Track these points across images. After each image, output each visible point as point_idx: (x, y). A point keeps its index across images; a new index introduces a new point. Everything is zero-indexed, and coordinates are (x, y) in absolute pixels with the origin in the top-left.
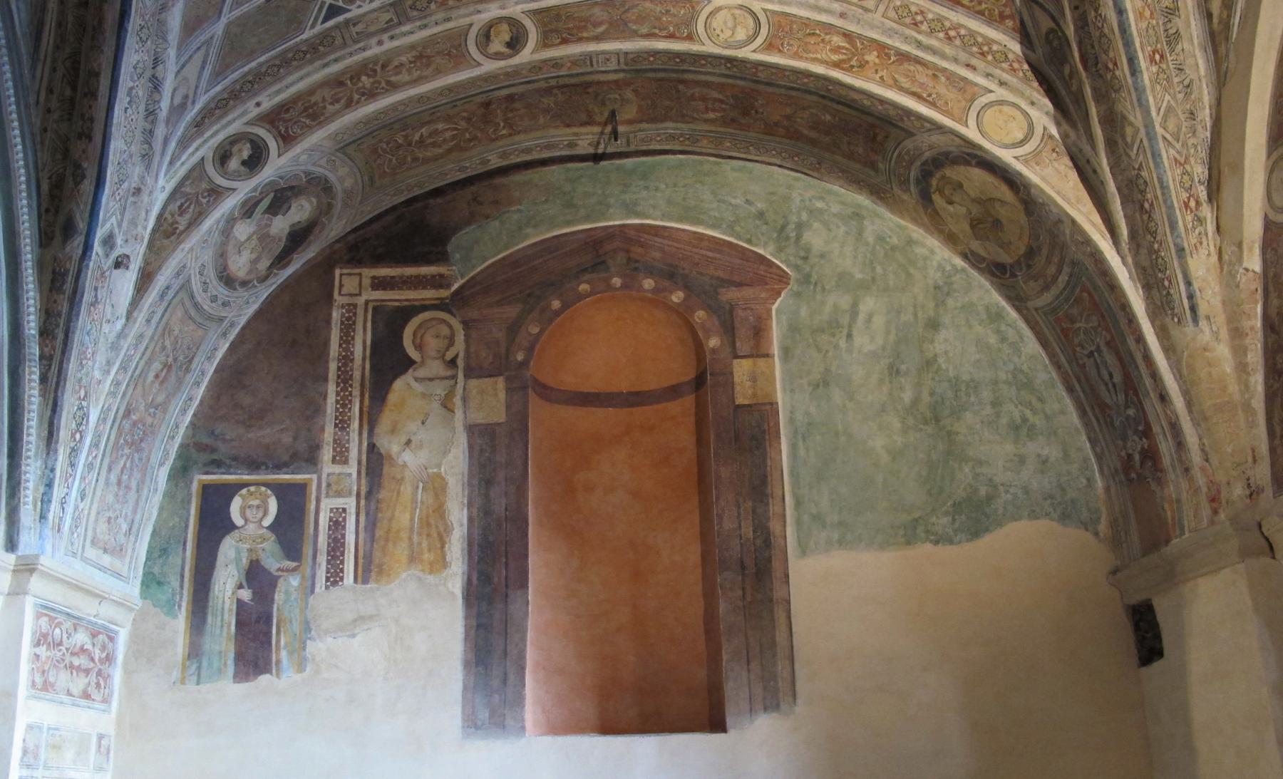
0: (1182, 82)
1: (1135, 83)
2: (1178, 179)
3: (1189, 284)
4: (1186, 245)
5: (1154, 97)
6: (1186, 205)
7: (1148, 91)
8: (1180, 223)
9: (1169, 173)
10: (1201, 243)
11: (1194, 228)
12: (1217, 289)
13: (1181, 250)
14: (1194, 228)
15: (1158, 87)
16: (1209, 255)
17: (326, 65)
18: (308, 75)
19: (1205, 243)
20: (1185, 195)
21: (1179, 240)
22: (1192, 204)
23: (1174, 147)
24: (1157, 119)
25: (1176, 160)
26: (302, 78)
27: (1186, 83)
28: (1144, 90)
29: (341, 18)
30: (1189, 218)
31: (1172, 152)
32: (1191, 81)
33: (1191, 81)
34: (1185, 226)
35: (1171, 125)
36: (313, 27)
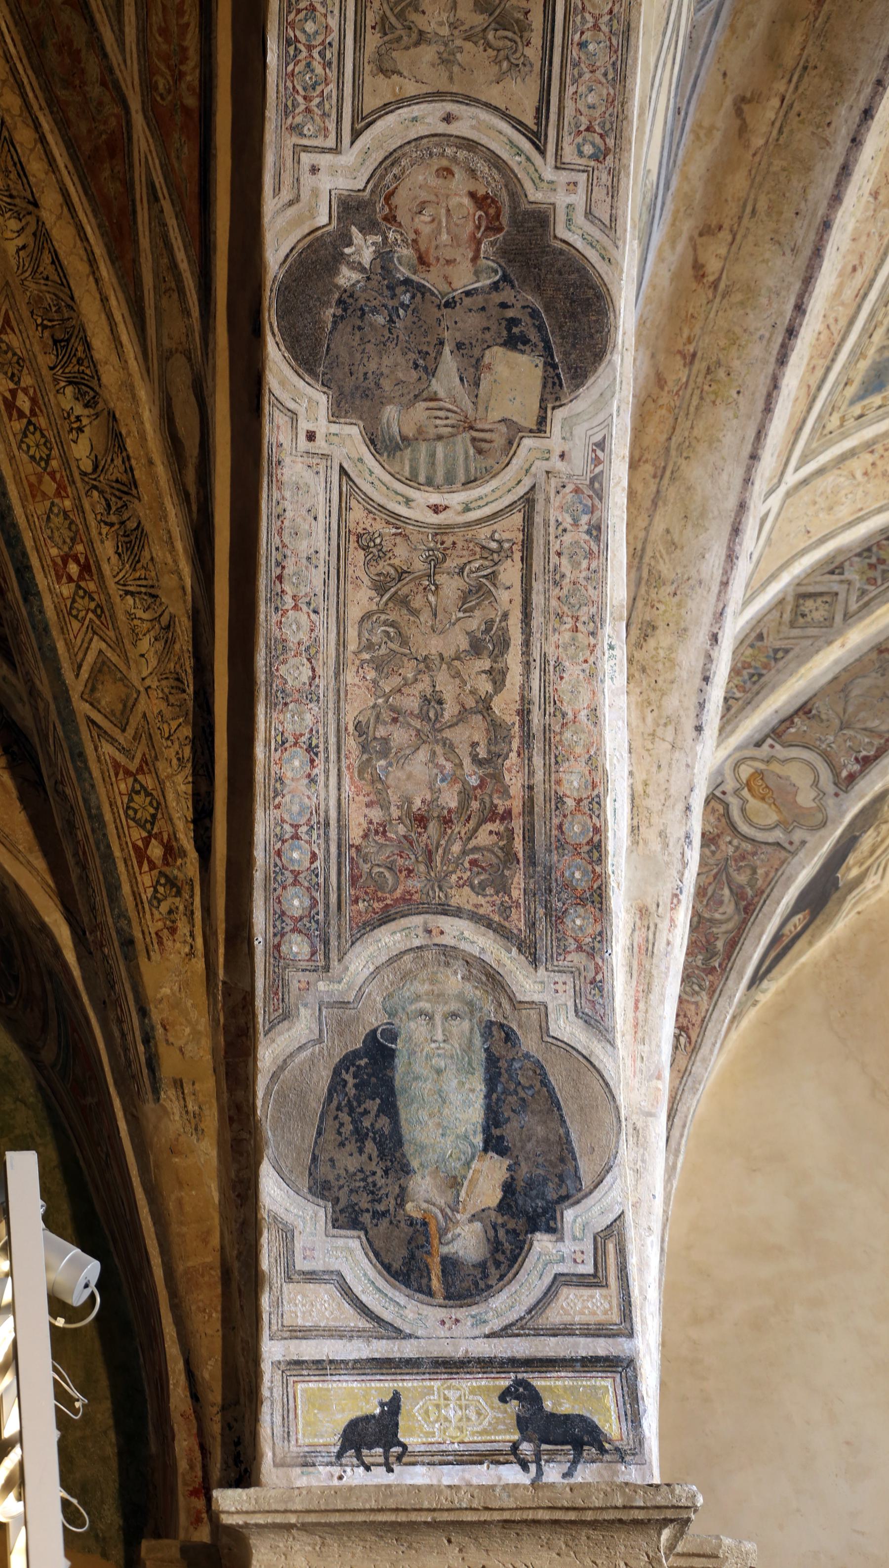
0: (158, 619)
1: (31, 614)
2: (121, 802)
3: (143, 1012)
4: (138, 935)
5: (68, 644)
6: (141, 854)
7: (55, 633)
8: (126, 889)
9: (102, 790)
10: (173, 931)
11: (156, 900)
12: (203, 1024)
13: (128, 943)
14: (156, 900)
15: (76, 625)
16: (191, 954)
19: (183, 928)
20: (137, 835)
21: (123, 923)
22: (156, 851)
23: (113, 741)
24: (76, 686)
25: (117, 765)
27: (165, 620)
28: (46, 630)
30: (146, 880)
31: (107, 749)
32: (172, 617)
33: (172, 617)
34: (136, 895)
35: (108, 695)
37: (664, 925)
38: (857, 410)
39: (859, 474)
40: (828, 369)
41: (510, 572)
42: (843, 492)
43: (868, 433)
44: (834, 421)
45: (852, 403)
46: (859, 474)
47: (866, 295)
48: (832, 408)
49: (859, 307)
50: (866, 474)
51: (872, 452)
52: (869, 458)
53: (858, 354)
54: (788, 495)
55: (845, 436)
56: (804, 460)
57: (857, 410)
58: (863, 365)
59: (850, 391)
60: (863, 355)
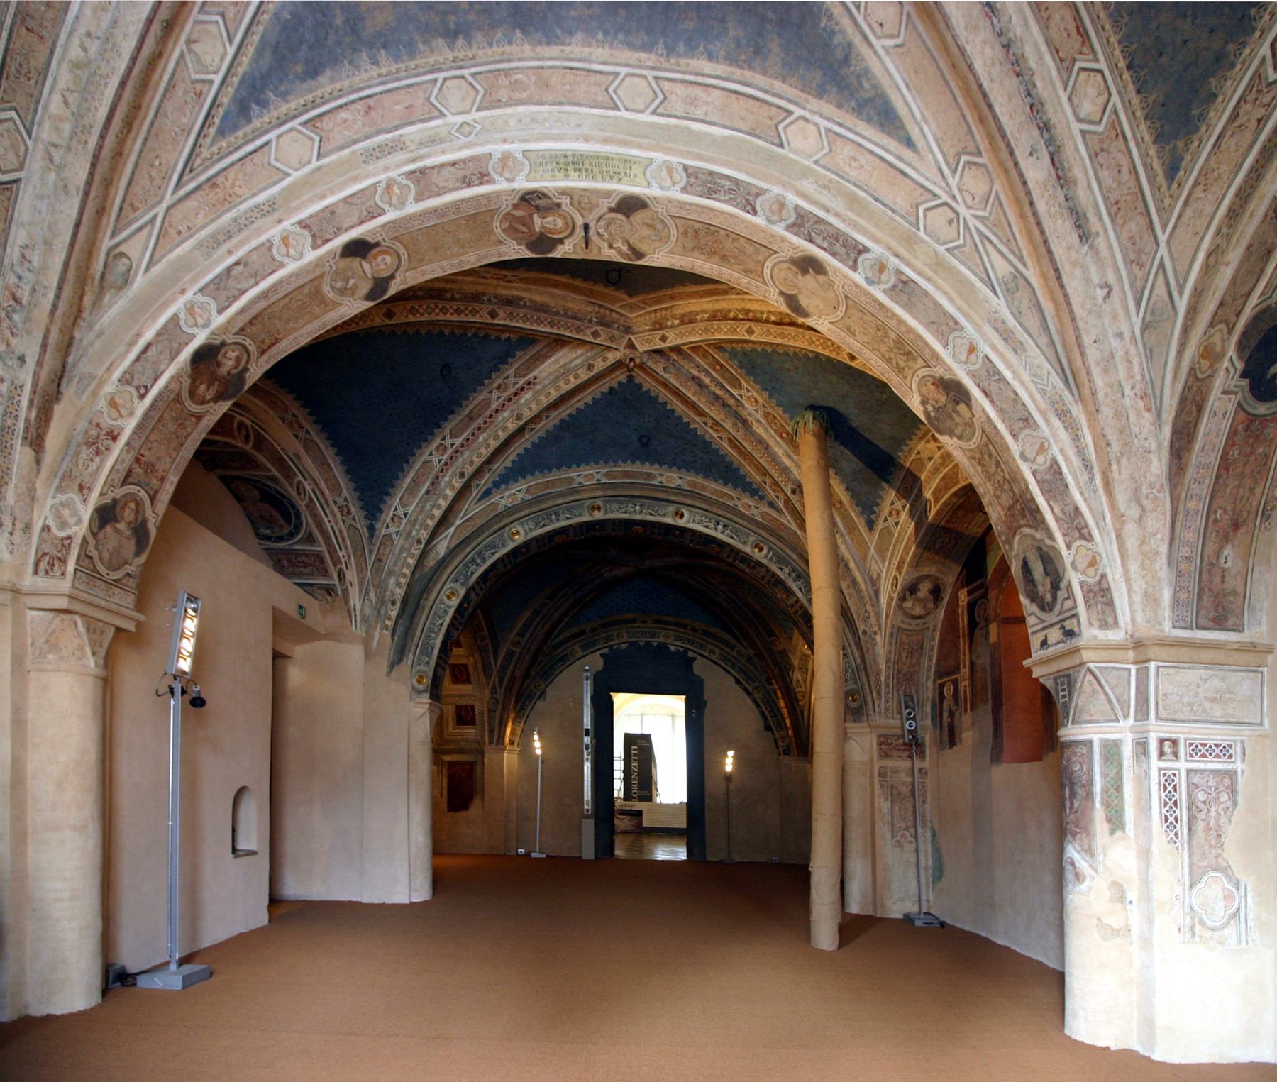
44: (1167, 201)
45: (1169, 188)
48: (1159, 201)
53: (1151, 181)
57: (1175, 186)
59: (1164, 188)
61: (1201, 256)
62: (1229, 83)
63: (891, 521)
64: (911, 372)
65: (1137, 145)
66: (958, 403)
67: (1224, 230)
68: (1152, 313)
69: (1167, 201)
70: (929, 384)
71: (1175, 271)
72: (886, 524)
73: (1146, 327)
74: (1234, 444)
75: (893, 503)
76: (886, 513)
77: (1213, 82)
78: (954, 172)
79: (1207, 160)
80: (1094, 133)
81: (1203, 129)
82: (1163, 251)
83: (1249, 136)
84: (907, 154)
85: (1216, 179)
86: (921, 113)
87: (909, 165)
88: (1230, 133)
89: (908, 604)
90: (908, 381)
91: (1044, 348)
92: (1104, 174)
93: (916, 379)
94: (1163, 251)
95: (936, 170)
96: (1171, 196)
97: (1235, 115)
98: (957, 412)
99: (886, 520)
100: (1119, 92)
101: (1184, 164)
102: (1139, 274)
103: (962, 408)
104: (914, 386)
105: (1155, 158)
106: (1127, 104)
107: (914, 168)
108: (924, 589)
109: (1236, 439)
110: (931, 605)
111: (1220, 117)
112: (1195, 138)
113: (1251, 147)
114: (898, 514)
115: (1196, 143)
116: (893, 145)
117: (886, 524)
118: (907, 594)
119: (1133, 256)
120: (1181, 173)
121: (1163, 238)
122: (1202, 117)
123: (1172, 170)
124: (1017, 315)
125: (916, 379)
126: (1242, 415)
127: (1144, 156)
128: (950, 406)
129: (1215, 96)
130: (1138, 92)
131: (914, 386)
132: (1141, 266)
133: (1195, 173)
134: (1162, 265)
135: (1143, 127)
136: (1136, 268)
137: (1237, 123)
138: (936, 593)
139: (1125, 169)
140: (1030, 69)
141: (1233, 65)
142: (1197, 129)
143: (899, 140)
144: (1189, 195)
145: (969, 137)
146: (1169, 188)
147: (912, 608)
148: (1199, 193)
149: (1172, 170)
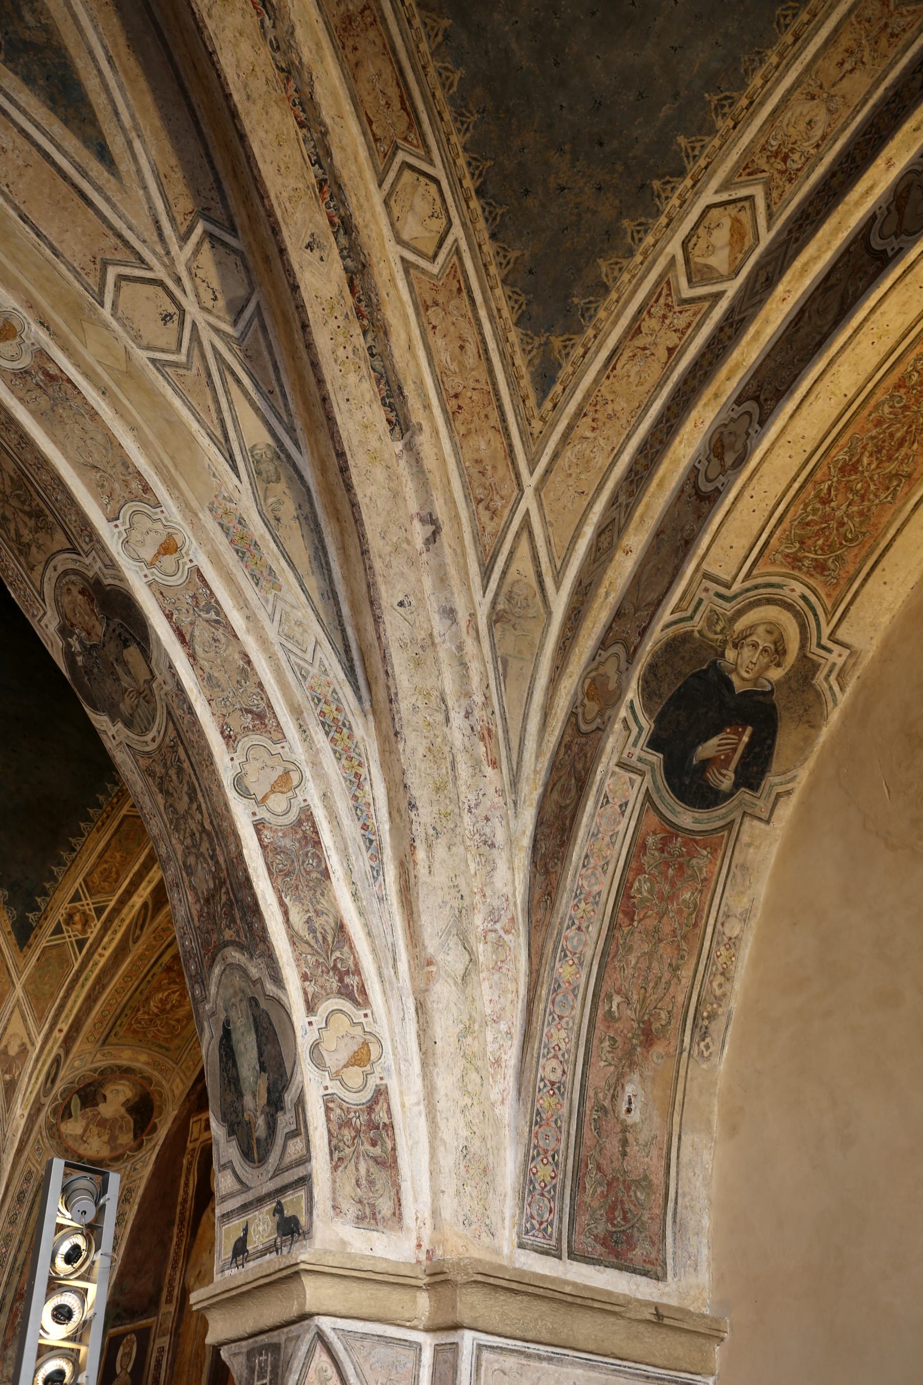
17: (83, 986)
18: (78, 997)
26: (75, 1001)
29: (87, 945)
36: (76, 959)
37: (411, 867)
38: (548, 405)
39: (588, 434)
40: (500, 407)
41: (181, 751)
42: (588, 452)
43: (571, 408)
44: (537, 425)
45: (539, 405)
46: (588, 434)
47: (486, 351)
48: (525, 421)
49: (489, 360)
50: (594, 429)
51: (585, 415)
52: (588, 420)
53: (513, 381)
54: (538, 490)
55: (554, 425)
56: (532, 465)
57: (548, 405)
58: (526, 382)
59: (532, 402)
60: (519, 378)
61: (589, 531)
62: (626, 277)
63: (71, 934)
64: (42, 557)
65: (491, 318)
66: (126, 644)
67: (623, 499)
68: (510, 598)
69: (537, 425)
70: (75, 591)
71: (548, 542)
72: (57, 940)
73: (496, 618)
74: (640, 870)
75: (76, 898)
76: (60, 915)
77: (604, 266)
78: (184, 238)
79: (596, 381)
80: (424, 271)
81: (590, 332)
82: (529, 502)
83: (655, 371)
84: (96, 168)
85: (609, 417)
86: (133, 117)
87: (99, 189)
88: (627, 353)
89: (73, 1128)
90: (36, 575)
91: (316, 597)
92: (439, 343)
93: (51, 575)
94: (529, 502)
95: (149, 221)
96: (542, 419)
97: (634, 330)
98: (125, 664)
99: (58, 930)
100: (464, 225)
101: (561, 375)
102: (490, 527)
103: (132, 653)
104: (48, 589)
105: (517, 348)
106: (476, 249)
107: (108, 200)
108: (116, 1100)
109: (644, 860)
110: (126, 1139)
111: (614, 323)
112: (579, 340)
113: (660, 385)
114: (86, 923)
115: (581, 351)
116: (72, 143)
117: (57, 940)
118: (76, 1102)
119: (480, 492)
120: (558, 388)
121: (530, 481)
122: (588, 313)
123: (545, 378)
124: (272, 522)
125: (51, 575)
126: (653, 820)
127: (502, 339)
128: (111, 647)
129: (607, 290)
130: (493, 236)
131: (48, 589)
132: (494, 514)
133: (578, 396)
134: (526, 524)
135: (499, 292)
136: (485, 516)
137: (640, 341)
138: (143, 1112)
139: (471, 348)
140: (322, 124)
141: (631, 253)
142: (580, 331)
143: (86, 141)
144: (570, 428)
145: (214, 194)
146: (539, 405)
147: (82, 1139)
148: (584, 427)
149: (545, 378)
